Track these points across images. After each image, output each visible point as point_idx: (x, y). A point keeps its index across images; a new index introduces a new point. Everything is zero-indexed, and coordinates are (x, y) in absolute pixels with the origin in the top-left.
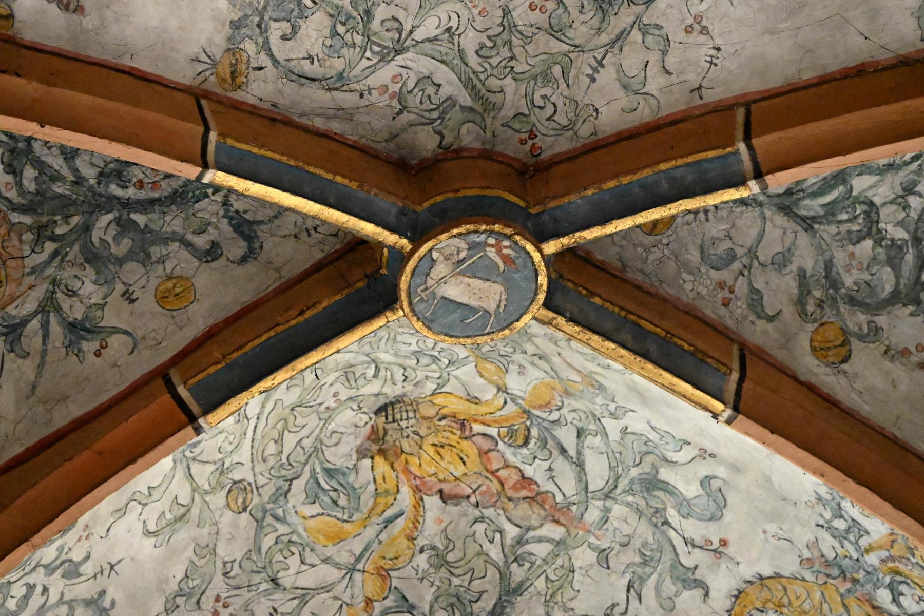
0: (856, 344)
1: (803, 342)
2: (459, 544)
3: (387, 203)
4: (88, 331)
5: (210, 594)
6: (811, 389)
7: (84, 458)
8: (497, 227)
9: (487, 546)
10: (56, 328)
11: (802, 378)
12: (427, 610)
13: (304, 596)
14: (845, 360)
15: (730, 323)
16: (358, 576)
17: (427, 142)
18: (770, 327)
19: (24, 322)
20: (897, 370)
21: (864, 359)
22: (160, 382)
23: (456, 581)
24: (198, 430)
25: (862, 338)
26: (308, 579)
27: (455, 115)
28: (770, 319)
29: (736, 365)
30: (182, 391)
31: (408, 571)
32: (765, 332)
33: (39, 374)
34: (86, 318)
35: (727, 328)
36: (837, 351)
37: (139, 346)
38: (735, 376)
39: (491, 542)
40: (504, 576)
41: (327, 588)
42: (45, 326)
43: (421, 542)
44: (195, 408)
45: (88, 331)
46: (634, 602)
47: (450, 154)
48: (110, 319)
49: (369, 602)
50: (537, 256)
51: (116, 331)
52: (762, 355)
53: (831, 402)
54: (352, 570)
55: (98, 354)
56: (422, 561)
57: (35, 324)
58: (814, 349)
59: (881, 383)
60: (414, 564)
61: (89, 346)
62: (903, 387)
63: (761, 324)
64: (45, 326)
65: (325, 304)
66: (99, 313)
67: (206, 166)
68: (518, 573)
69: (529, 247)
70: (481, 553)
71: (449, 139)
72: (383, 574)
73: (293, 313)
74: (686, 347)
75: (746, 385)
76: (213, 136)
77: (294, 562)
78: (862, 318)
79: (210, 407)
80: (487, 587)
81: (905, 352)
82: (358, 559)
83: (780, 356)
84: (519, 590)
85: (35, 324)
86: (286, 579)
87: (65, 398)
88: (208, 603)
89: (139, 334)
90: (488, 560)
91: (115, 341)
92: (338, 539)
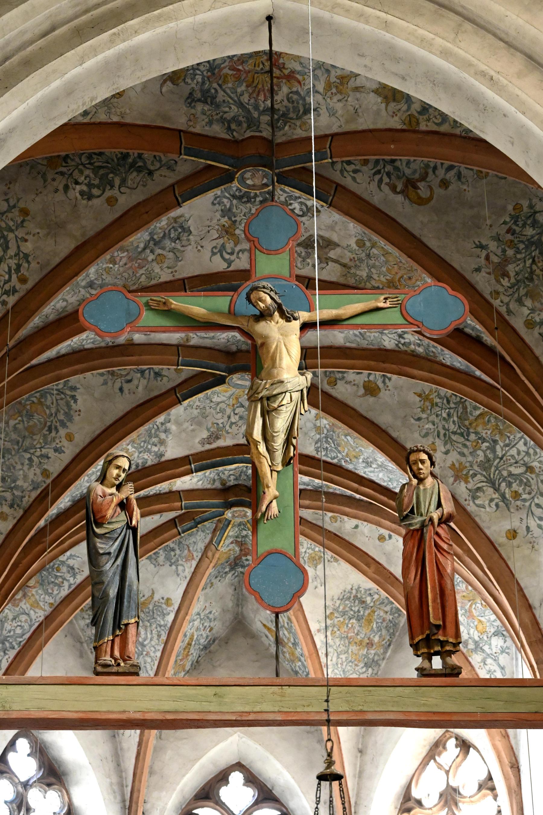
0: (338, 381)
1: (326, 382)
3: (223, 366)
5: (196, 404)
13: (218, 404)
16: (231, 400)
17: (234, 348)
19: (145, 370)
20: (348, 386)
22: (173, 391)
25: (340, 379)
26: (219, 400)
27: (240, 343)
30: (178, 395)
33: (148, 383)
41: (223, 402)
42: (150, 372)
44: (181, 399)
47: (239, 351)
48: (164, 373)
51: (165, 376)
54: (230, 398)
57: (147, 371)
59: (344, 390)
61: (159, 379)
62: (349, 390)
64: (150, 372)
67: (178, 366)
71: (239, 347)
72: (237, 399)
76: (180, 358)
77: (216, 396)
78: (340, 375)
79: (184, 400)
81: (351, 382)
85: (147, 371)
86: (214, 400)
88: (194, 407)
91: (165, 378)
92: (226, 391)
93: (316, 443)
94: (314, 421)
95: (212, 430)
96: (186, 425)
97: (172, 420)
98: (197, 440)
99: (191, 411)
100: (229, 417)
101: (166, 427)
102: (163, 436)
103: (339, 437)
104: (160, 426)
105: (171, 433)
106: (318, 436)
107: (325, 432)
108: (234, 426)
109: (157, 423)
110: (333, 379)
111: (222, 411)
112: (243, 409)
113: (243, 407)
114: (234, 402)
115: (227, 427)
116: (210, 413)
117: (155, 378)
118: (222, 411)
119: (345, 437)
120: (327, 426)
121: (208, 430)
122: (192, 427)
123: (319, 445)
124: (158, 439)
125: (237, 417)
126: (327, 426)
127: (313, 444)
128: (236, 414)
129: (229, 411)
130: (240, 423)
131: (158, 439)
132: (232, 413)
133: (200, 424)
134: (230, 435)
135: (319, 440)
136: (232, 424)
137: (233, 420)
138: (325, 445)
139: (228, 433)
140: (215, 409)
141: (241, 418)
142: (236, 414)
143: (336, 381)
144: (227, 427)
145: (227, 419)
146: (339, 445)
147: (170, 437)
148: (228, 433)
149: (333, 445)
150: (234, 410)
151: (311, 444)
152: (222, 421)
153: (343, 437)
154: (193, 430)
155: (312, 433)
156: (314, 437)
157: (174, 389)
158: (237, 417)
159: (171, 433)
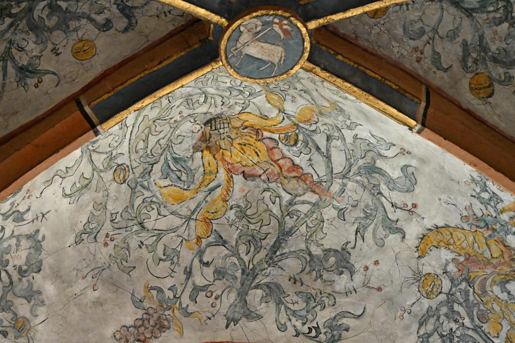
1: (465, 84)
2: (254, 204)
4: (31, 72)
5: (103, 232)
6: (468, 112)
7: (27, 149)
8: (280, 12)
9: (271, 205)
10: (11, 70)
11: (464, 106)
12: (234, 244)
13: (160, 234)
14: (490, 96)
15: (421, 73)
16: (192, 223)
18: (445, 75)
21: (501, 95)
23: (252, 227)
24: (97, 133)
25: (500, 82)
26: (162, 224)
28: (446, 70)
29: (424, 98)
30: (87, 109)
31: (223, 220)
32: (442, 78)
34: (30, 64)
35: (418, 75)
36: (486, 90)
37: (62, 82)
38: (423, 104)
39: (274, 203)
40: (281, 224)
41: (174, 230)
43: (231, 203)
44: (95, 120)
45: (31, 72)
46: (360, 241)
48: (44, 66)
49: (199, 239)
50: (304, 30)
51: (47, 72)
52: (440, 92)
53: (481, 121)
54: (189, 219)
55: (36, 86)
56: (231, 214)
58: (471, 89)
60: (226, 216)
61: (31, 81)
63: (440, 73)
65: (175, 57)
66: (37, 61)
68: (289, 222)
69: (299, 25)
70: (268, 210)
72: (208, 222)
73: (156, 63)
74: (394, 86)
75: (430, 110)
77: (154, 214)
78: (501, 70)
79: (104, 120)
80: (271, 230)
82: (193, 213)
83: (451, 93)
84: (290, 233)
86: (149, 224)
87: (16, 113)
88: (101, 238)
89: (62, 74)
90: (272, 214)
91: (46, 78)
92: (181, 200)
93: (421, 325)
94: (413, 263)
95: (146, 304)
96: (79, 286)
97: (45, 266)
98: (109, 331)
99: (92, 246)
100: (189, 273)
101: (31, 285)
102: (23, 308)
103: (484, 292)
104: (15, 276)
105: (43, 303)
106: (426, 303)
107: (446, 285)
108: (202, 294)
109: (10, 268)
110: (483, 80)
111: (171, 256)
112: (223, 251)
113: (224, 243)
114: (201, 229)
115: (185, 300)
116: (140, 259)
117: (21, 81)
118: (171, 256)
119: (504, 290)
120: (452, 268)
121: (138, 303)
122: (96, 294)
123: (430, 327)
124: (10, 316)
125: (209, 271)
126: (452, 268)
127: (415, 327)
128: (207, 264)
129: (187, 256)
130: (218, 287)
131: (10, 316)
132: (196, 262)
133: (115, 285)
134: (192, 320)
135: (430, 314)
136: (197, 289)
137: (199, 281)
138: (448, 325)
139: (188, 314)
140: (152, 249)
141: (220, 273)
142: (207, 264)
143: (491, 85)
144: (185, 300)
145: (183, 277)
146: (483, 318)
147: (42, 312)
148: (188, 314)
149: (467, 322)
150: (201, 253)
151: (407, 327)
152: (169, 282)
153: (497, 290)
154: (98, 303)
155: (410, 297)
156: (415, 309)
157: (75, 100)
158: (209, 271)
159: (43, 303)
